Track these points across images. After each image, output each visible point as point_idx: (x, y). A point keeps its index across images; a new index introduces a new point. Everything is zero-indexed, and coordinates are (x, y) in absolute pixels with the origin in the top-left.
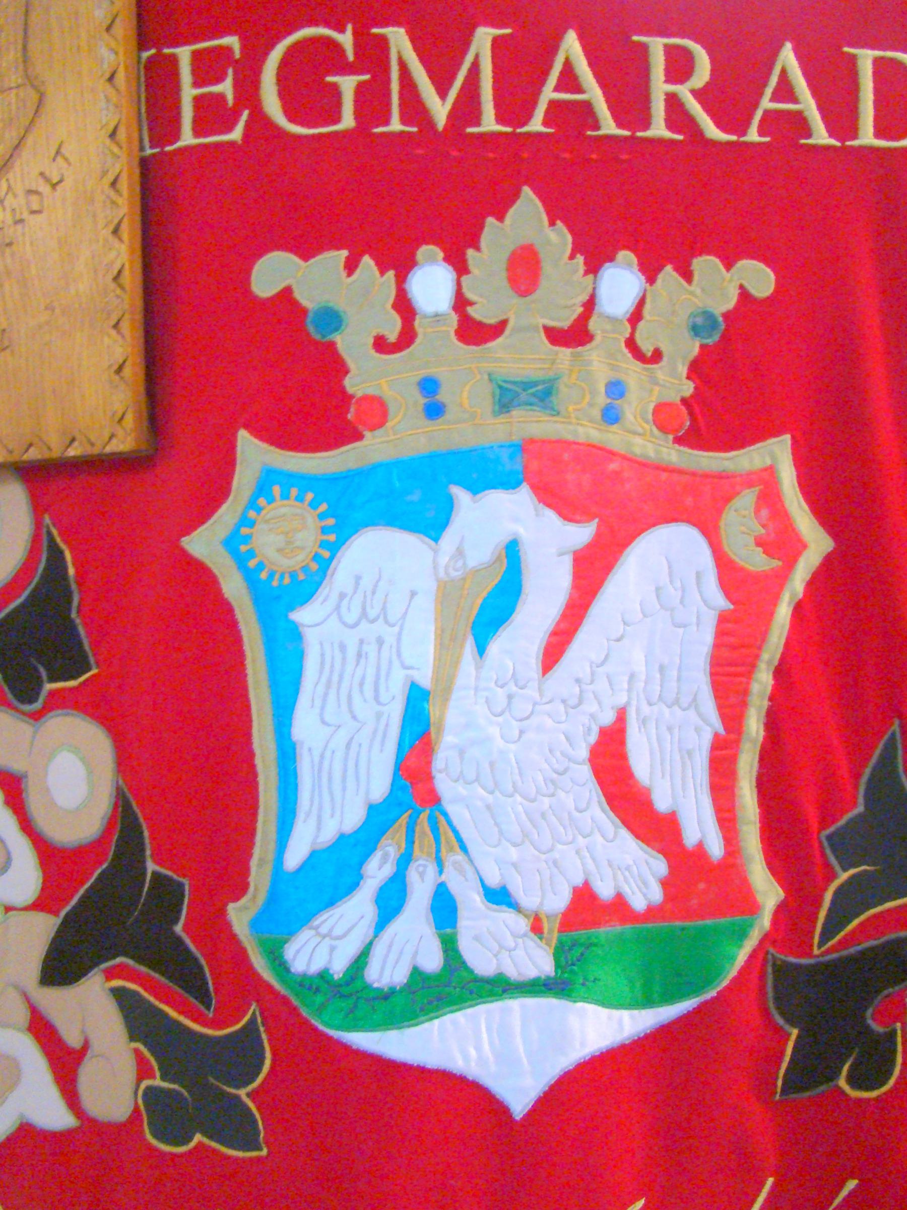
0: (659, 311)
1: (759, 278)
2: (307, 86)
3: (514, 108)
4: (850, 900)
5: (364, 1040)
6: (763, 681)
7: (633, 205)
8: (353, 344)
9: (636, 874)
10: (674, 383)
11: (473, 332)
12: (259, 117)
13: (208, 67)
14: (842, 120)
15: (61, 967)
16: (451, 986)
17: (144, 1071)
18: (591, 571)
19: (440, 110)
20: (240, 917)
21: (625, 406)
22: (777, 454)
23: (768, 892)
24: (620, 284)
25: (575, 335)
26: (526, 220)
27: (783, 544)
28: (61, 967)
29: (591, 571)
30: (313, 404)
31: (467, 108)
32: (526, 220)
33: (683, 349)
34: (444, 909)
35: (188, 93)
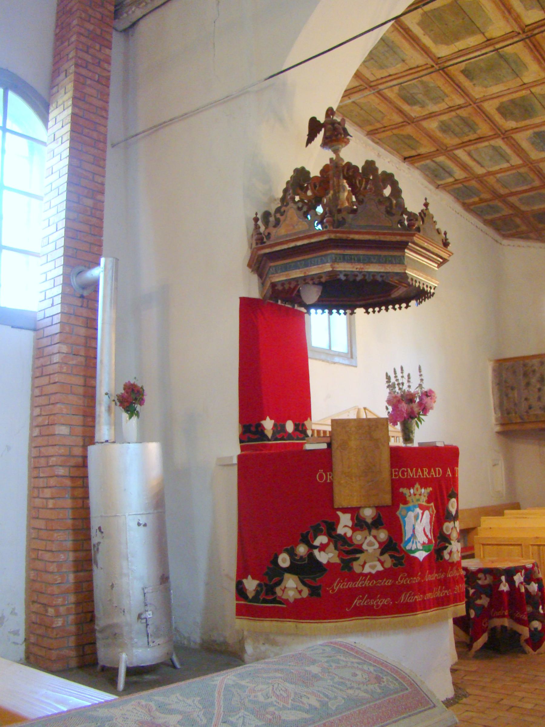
0: (425, 491)
1: (431, 489)
2: (403, 475)
3: (416, 476)
4: (439, 543)
5: (412, 555)
6: (433, 523)
7: (424, 483)
8: (407, 496)
9: (426, 540)
10: (426, 498)
11: (415, 495)
12: (399, 477)
13: (395, 471)
14: (436, 475)
15: (382, 554)
16: (417, 550)
17: (392, 561)
18: (423, 514)
19: (412, 475)
20: (402, 545)
21: (423, 500)
22: (432, 504)
23: (434, 542)
24: (423, 490)
25: (420, 495)
26: (417, 486)
27: (433, 512)
28: (382, 554)
29: (423, 514)
30: (406, 502)
31: (413, 475)
32: (417, 486)
33: (426, 495)
34: (416, 543)
35: (393, 473)
